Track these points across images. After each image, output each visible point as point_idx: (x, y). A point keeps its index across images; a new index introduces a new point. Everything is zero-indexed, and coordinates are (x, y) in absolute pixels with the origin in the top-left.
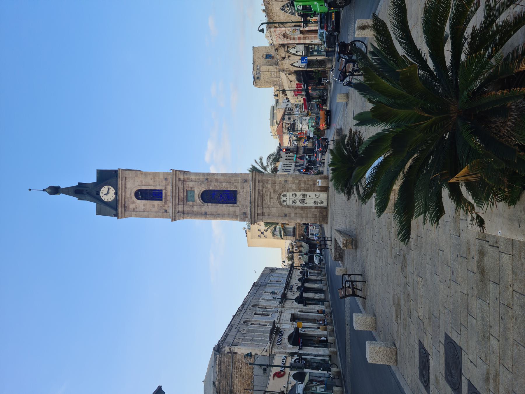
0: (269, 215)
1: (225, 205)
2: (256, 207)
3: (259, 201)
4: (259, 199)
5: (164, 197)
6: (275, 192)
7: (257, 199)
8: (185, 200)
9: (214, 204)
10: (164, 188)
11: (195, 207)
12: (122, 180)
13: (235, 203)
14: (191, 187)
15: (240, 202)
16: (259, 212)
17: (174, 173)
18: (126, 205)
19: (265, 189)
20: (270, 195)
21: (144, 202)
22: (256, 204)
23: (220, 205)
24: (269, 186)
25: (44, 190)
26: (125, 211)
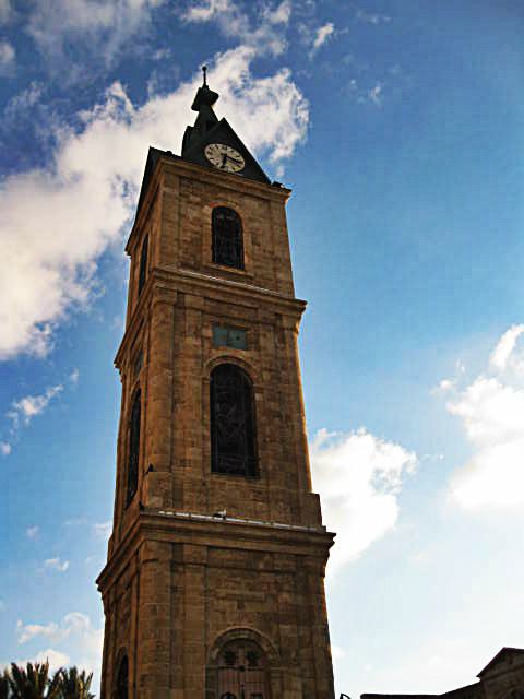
0: (174, 589)
1: (208, 433)
2: (208, 542)
3: (228, 555)
4: (237, 556)
5: (222, 268)
6: (268, 620)
7: (239, 545)
8: (217, 320)
9: (208, 398)
10: (249, 274)
11: (199, 343)
12: (262, 191)
13: (217, 469)
14: (257, 342)
15: (224, 483)
16: (187, 550)
17: (298, 305)
18: (196, 184)
19: (270, 578)
20: (252, 600)
21: (210, 221)
22: (219, 542)
23: (207, 417)
24: (285, 596)
25: (205, 86)
26: (181, 177)
